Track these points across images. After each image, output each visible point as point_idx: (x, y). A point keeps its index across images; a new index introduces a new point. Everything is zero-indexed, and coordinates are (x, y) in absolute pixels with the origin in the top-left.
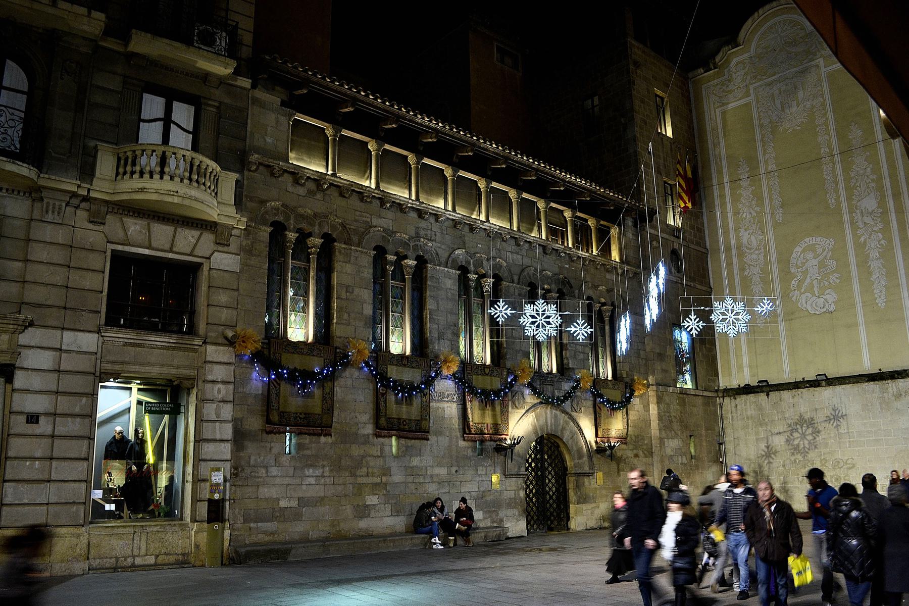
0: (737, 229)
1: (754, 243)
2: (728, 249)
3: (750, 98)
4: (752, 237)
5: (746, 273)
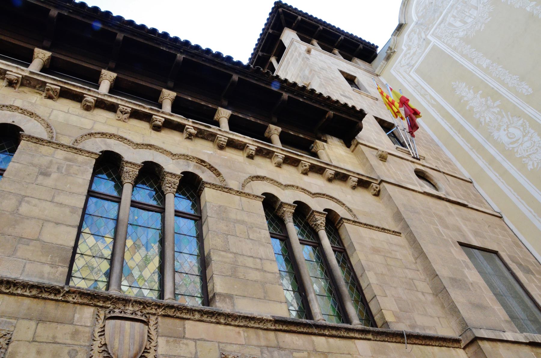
0: (489, 137)
1: (518, 133)
2: (492, 161)
3: (432, 43)
4: (511, 130)
5: (530, 167)
